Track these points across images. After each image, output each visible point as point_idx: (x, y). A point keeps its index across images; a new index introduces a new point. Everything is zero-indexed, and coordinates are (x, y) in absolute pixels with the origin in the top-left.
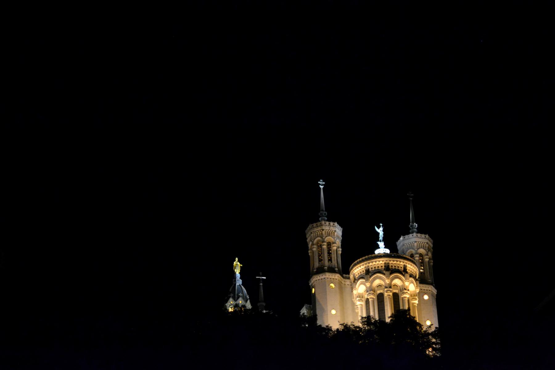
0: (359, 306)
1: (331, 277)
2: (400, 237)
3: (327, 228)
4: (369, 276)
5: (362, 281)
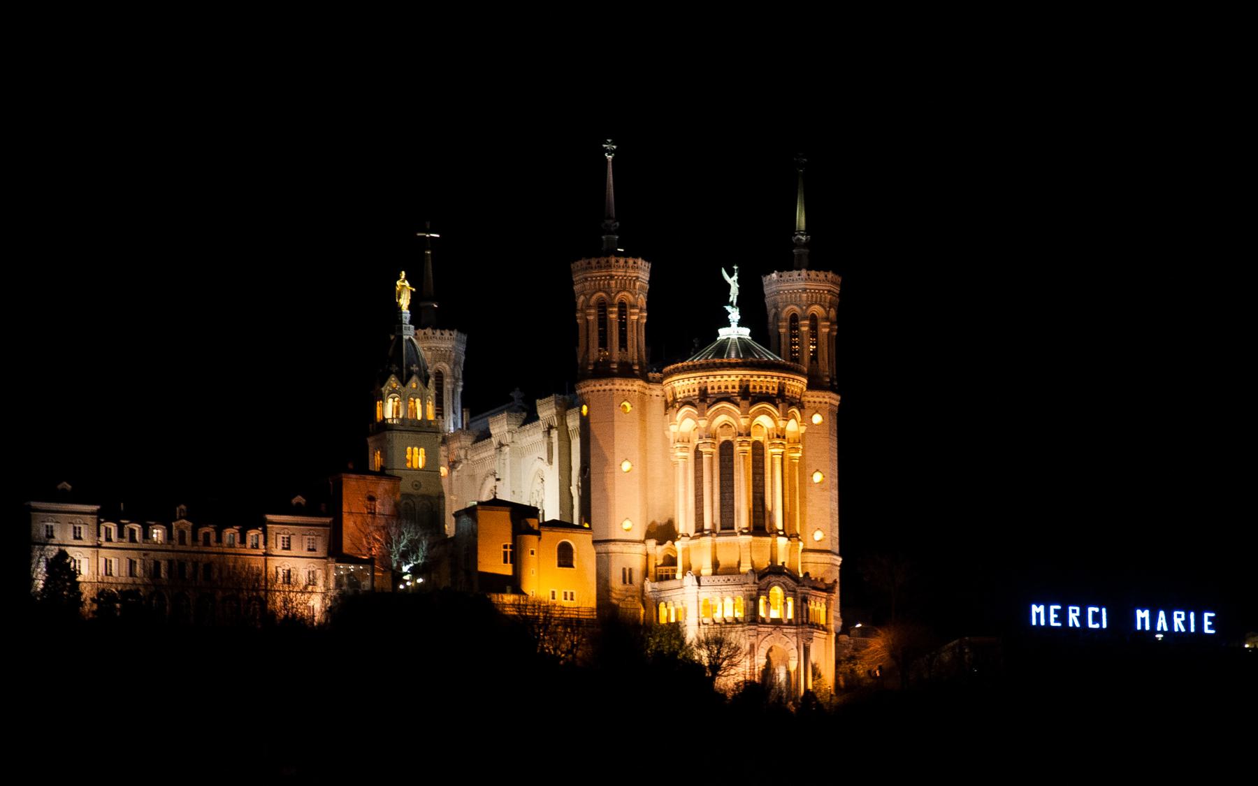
0: (680, 461)
1: (624, 387)
2: (773, 272)
3: (621, 272)
4: (706, 405)
5: (689, 411)
